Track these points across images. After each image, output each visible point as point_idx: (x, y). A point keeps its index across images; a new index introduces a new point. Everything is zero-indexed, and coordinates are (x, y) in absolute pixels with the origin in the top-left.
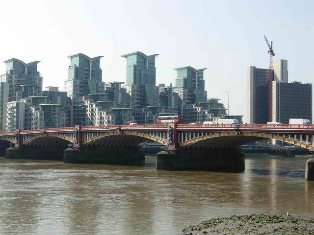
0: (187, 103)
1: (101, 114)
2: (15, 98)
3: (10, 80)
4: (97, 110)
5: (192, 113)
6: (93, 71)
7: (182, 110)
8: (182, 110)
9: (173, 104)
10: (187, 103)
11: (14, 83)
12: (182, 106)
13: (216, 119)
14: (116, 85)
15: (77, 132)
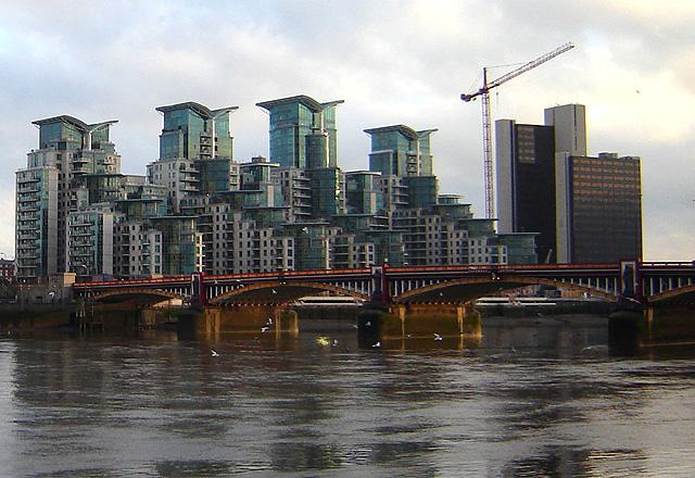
0: (398, 206)
1: (257, 235)
2: (74, 203)
3: (58, 162)
4: (246, 225)
5: (414, 229)
6: (216, 139)
7: (390, 221)
8: (390, 221)
9: (374, 211)
10: (398, 206)
11: (68, 169)
12: (390, 214)
13: (476, 243)
14: (255, 167)
15: (377, 276)
